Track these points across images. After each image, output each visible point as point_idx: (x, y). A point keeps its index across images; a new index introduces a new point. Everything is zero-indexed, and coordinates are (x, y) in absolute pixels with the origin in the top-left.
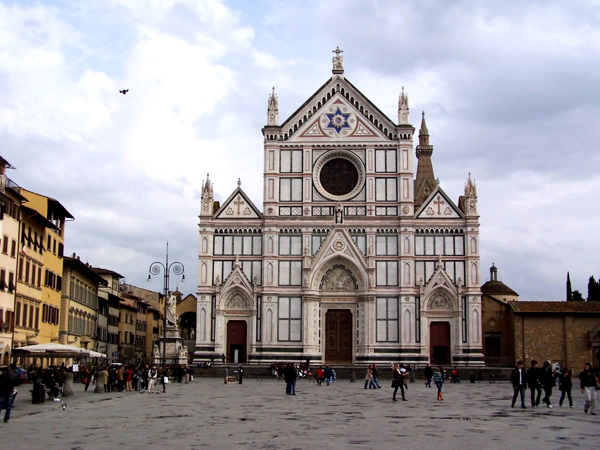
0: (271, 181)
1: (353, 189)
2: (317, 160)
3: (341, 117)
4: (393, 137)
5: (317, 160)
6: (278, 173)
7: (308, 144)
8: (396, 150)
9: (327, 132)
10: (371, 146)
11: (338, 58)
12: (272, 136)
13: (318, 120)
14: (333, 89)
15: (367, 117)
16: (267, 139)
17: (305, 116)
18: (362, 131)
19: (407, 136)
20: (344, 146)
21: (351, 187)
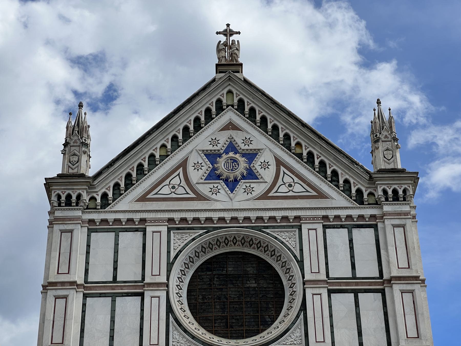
0: (61, 303)
1: (273, 322)
2: (180, 251)
3: (237, 156)
4: (365, 196)
5: (180, 251)
6: (81, 281)
7: (160, 215)
8: (375, 227)
9: (204, 189)
10: (314, 219)
11: (225, 44)
12: (69, 197)
13: (183, 164)
14: (219, 102)
15: (300, 156)
16: (56, 204)
17: (152, 156)
18: (290, 186)
19: (401, 192)
20: (247, 219)
21: (268, 320)
